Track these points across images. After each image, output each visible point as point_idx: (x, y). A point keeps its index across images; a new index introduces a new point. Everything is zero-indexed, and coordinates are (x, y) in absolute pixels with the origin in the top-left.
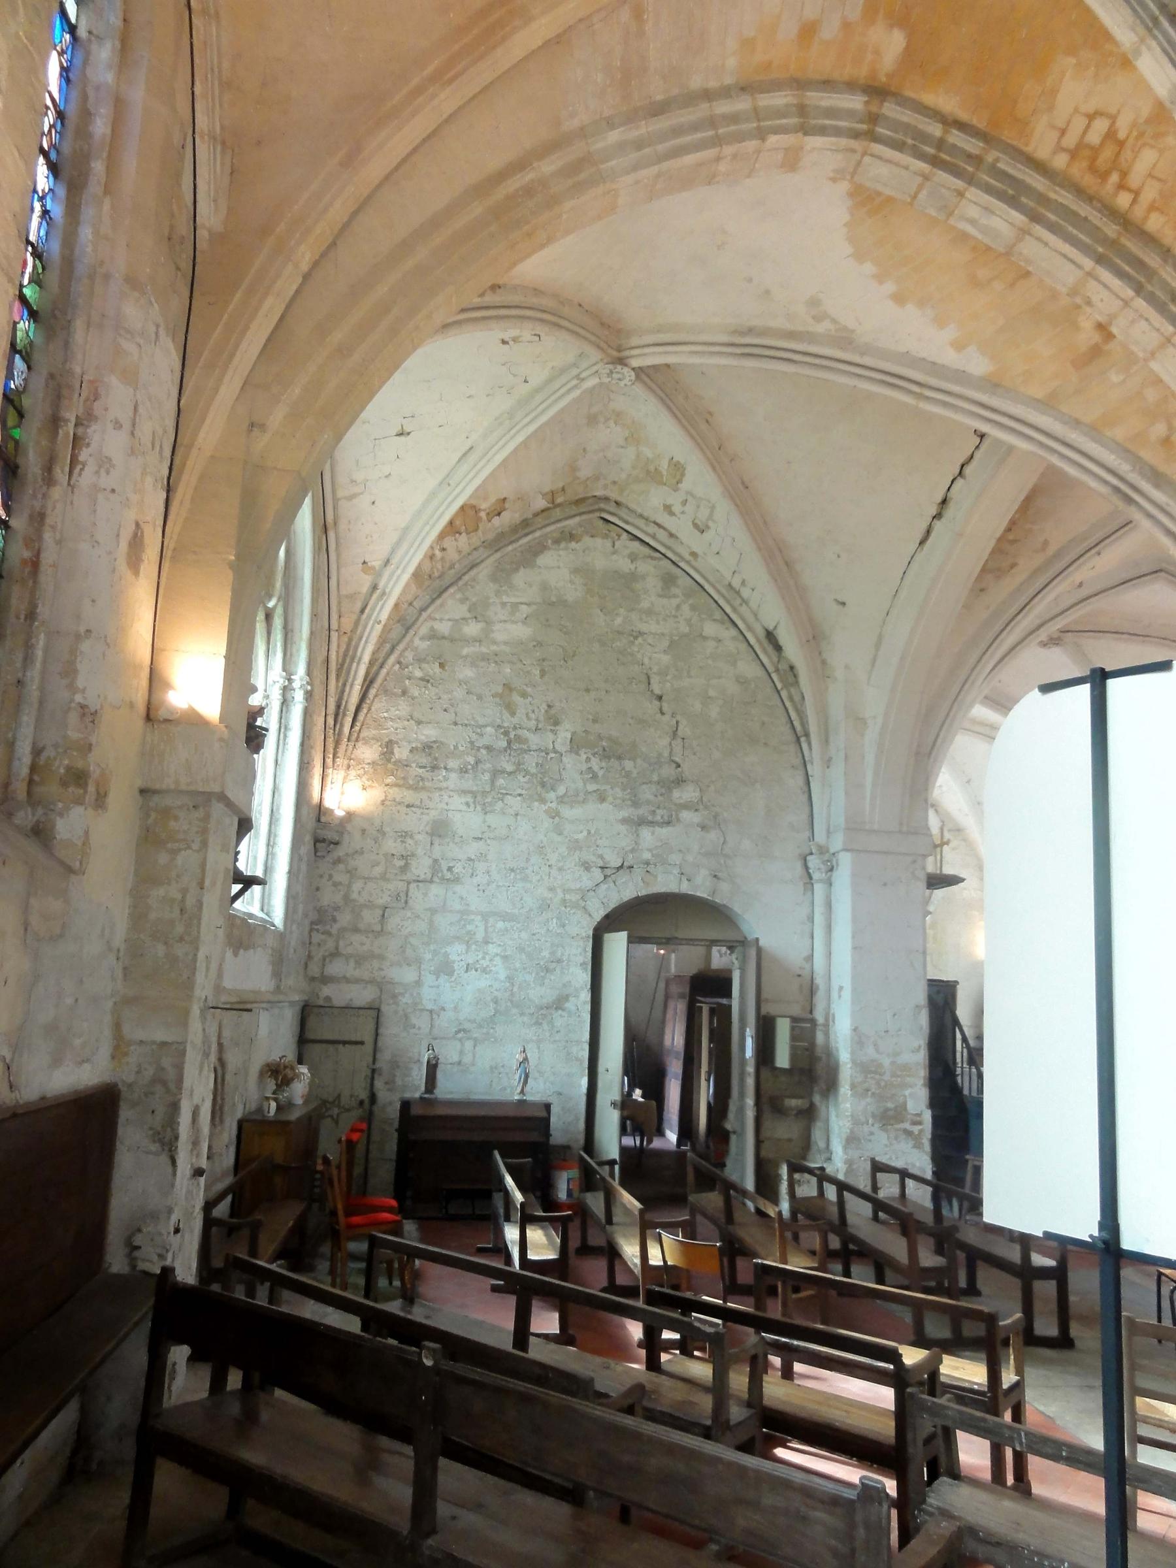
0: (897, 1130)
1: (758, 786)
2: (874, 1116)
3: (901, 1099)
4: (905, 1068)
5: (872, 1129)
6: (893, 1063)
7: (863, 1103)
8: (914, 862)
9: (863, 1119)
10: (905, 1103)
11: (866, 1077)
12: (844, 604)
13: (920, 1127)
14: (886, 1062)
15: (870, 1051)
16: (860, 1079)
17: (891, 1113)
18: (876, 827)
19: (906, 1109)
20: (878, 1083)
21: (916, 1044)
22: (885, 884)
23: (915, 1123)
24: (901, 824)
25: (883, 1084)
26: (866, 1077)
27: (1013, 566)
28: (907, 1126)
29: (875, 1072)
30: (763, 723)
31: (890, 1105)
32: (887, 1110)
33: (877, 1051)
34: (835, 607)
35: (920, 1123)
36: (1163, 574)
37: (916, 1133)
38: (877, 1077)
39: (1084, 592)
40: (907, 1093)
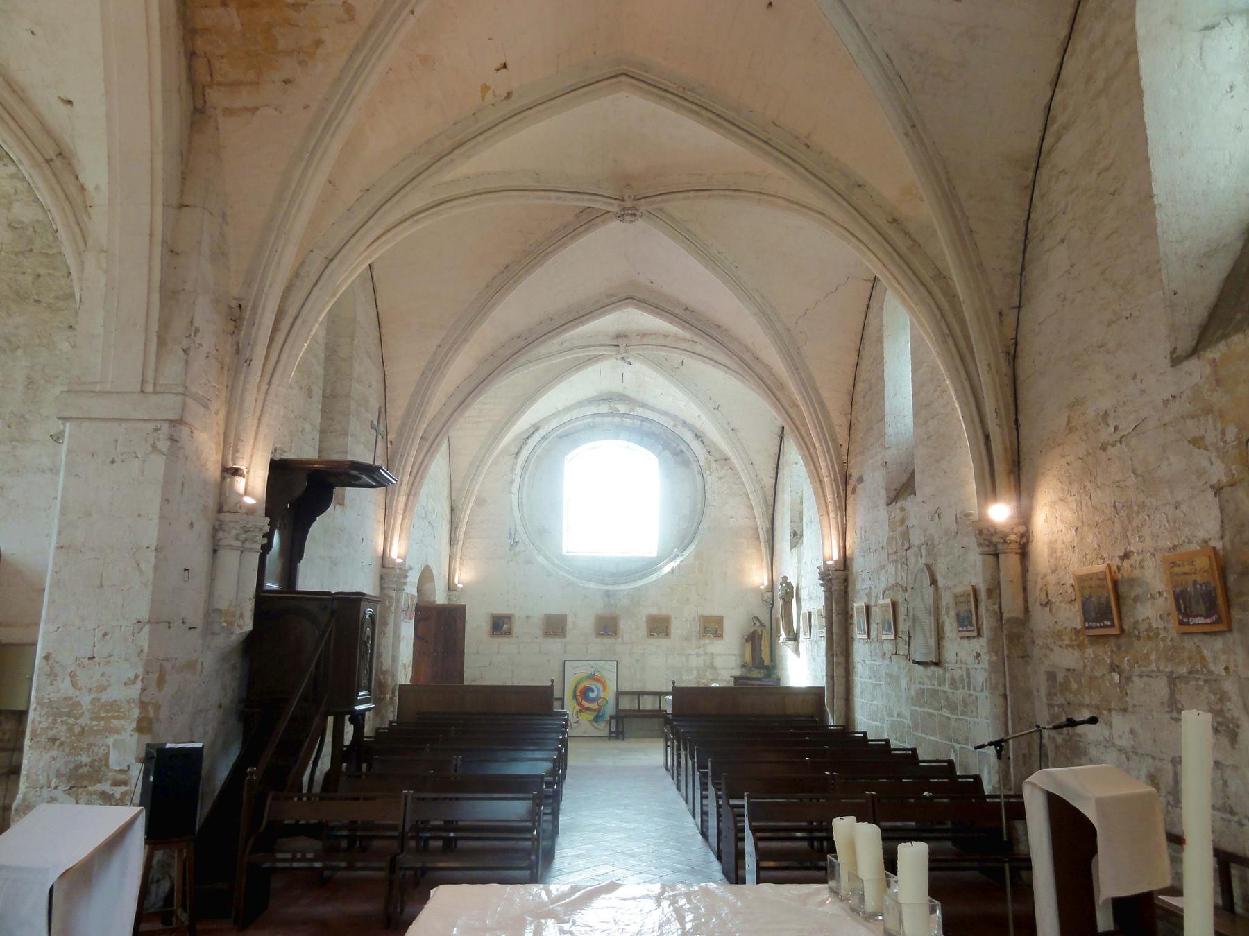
0: (90, 794)
1: (20, 353)
2: (59, 775)
3: (101, 751)
4: (113, 708)
5: (55, 793)
6: (95, 701)
7: (46, 757)
8: (156, 430)
9: (43, 780)
10: (107, 756)
11: (54, 722)
12: (70, 102)
13: (123, 789)
14: (85, 700)
15: (65, 687)
16: (44, 725)
17: (84, 770)
18: (108, 387)
19: (107, 765)
20: (70, 730)
21: (131, 675)
22: (113, 462)
23: (116, 783)
24: (143, 382)
25: (77, 730)
26: (54, 722)
27: (319, 43)
28: (106, 787)
29: (69, 715)
30: (39, 276)
31: (85, 759)
32: (78, 767)
33: (74, 685)
34: (64, 108)
35: (125, 783)
36: (623, 79)
37: (118, 796)
38: (71, 721)
39: (516, 103)
40: (110, 741)
